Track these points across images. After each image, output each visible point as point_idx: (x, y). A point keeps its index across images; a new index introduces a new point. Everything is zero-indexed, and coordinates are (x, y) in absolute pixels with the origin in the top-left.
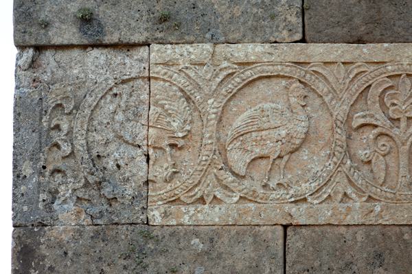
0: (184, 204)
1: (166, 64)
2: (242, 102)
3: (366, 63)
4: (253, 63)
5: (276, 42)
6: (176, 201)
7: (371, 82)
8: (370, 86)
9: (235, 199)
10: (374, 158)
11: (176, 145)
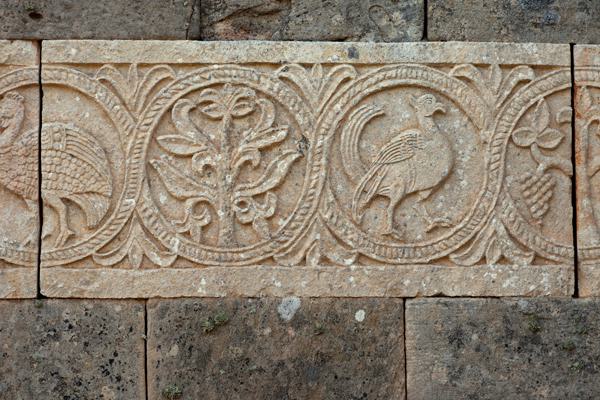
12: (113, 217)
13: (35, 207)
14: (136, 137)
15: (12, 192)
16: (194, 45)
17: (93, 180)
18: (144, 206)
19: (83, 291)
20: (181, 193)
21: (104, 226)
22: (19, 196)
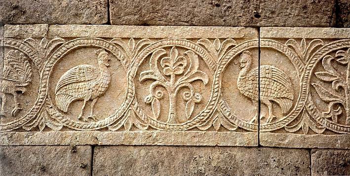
0: (25, 130)
1: (15, 38)
2: (66, 63)
3: (149, 38)
4: (75, 38)
5: (90, 24)
6: (20, 129)
7: (152, 51)
8: (152, 53)
9: (60, 128)
10: (153, 101)
11: (21, 92)
12: (294, 109)
13: (257, 104)
14: (305, 73)
15: (246, 97)
16: (333, 30)
17: (284, 92)
18: (309, 105)
19: (280, 144)
20: (327, 99)
21: (290, 114)
22: (249, 99)
